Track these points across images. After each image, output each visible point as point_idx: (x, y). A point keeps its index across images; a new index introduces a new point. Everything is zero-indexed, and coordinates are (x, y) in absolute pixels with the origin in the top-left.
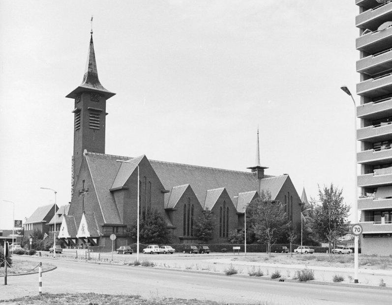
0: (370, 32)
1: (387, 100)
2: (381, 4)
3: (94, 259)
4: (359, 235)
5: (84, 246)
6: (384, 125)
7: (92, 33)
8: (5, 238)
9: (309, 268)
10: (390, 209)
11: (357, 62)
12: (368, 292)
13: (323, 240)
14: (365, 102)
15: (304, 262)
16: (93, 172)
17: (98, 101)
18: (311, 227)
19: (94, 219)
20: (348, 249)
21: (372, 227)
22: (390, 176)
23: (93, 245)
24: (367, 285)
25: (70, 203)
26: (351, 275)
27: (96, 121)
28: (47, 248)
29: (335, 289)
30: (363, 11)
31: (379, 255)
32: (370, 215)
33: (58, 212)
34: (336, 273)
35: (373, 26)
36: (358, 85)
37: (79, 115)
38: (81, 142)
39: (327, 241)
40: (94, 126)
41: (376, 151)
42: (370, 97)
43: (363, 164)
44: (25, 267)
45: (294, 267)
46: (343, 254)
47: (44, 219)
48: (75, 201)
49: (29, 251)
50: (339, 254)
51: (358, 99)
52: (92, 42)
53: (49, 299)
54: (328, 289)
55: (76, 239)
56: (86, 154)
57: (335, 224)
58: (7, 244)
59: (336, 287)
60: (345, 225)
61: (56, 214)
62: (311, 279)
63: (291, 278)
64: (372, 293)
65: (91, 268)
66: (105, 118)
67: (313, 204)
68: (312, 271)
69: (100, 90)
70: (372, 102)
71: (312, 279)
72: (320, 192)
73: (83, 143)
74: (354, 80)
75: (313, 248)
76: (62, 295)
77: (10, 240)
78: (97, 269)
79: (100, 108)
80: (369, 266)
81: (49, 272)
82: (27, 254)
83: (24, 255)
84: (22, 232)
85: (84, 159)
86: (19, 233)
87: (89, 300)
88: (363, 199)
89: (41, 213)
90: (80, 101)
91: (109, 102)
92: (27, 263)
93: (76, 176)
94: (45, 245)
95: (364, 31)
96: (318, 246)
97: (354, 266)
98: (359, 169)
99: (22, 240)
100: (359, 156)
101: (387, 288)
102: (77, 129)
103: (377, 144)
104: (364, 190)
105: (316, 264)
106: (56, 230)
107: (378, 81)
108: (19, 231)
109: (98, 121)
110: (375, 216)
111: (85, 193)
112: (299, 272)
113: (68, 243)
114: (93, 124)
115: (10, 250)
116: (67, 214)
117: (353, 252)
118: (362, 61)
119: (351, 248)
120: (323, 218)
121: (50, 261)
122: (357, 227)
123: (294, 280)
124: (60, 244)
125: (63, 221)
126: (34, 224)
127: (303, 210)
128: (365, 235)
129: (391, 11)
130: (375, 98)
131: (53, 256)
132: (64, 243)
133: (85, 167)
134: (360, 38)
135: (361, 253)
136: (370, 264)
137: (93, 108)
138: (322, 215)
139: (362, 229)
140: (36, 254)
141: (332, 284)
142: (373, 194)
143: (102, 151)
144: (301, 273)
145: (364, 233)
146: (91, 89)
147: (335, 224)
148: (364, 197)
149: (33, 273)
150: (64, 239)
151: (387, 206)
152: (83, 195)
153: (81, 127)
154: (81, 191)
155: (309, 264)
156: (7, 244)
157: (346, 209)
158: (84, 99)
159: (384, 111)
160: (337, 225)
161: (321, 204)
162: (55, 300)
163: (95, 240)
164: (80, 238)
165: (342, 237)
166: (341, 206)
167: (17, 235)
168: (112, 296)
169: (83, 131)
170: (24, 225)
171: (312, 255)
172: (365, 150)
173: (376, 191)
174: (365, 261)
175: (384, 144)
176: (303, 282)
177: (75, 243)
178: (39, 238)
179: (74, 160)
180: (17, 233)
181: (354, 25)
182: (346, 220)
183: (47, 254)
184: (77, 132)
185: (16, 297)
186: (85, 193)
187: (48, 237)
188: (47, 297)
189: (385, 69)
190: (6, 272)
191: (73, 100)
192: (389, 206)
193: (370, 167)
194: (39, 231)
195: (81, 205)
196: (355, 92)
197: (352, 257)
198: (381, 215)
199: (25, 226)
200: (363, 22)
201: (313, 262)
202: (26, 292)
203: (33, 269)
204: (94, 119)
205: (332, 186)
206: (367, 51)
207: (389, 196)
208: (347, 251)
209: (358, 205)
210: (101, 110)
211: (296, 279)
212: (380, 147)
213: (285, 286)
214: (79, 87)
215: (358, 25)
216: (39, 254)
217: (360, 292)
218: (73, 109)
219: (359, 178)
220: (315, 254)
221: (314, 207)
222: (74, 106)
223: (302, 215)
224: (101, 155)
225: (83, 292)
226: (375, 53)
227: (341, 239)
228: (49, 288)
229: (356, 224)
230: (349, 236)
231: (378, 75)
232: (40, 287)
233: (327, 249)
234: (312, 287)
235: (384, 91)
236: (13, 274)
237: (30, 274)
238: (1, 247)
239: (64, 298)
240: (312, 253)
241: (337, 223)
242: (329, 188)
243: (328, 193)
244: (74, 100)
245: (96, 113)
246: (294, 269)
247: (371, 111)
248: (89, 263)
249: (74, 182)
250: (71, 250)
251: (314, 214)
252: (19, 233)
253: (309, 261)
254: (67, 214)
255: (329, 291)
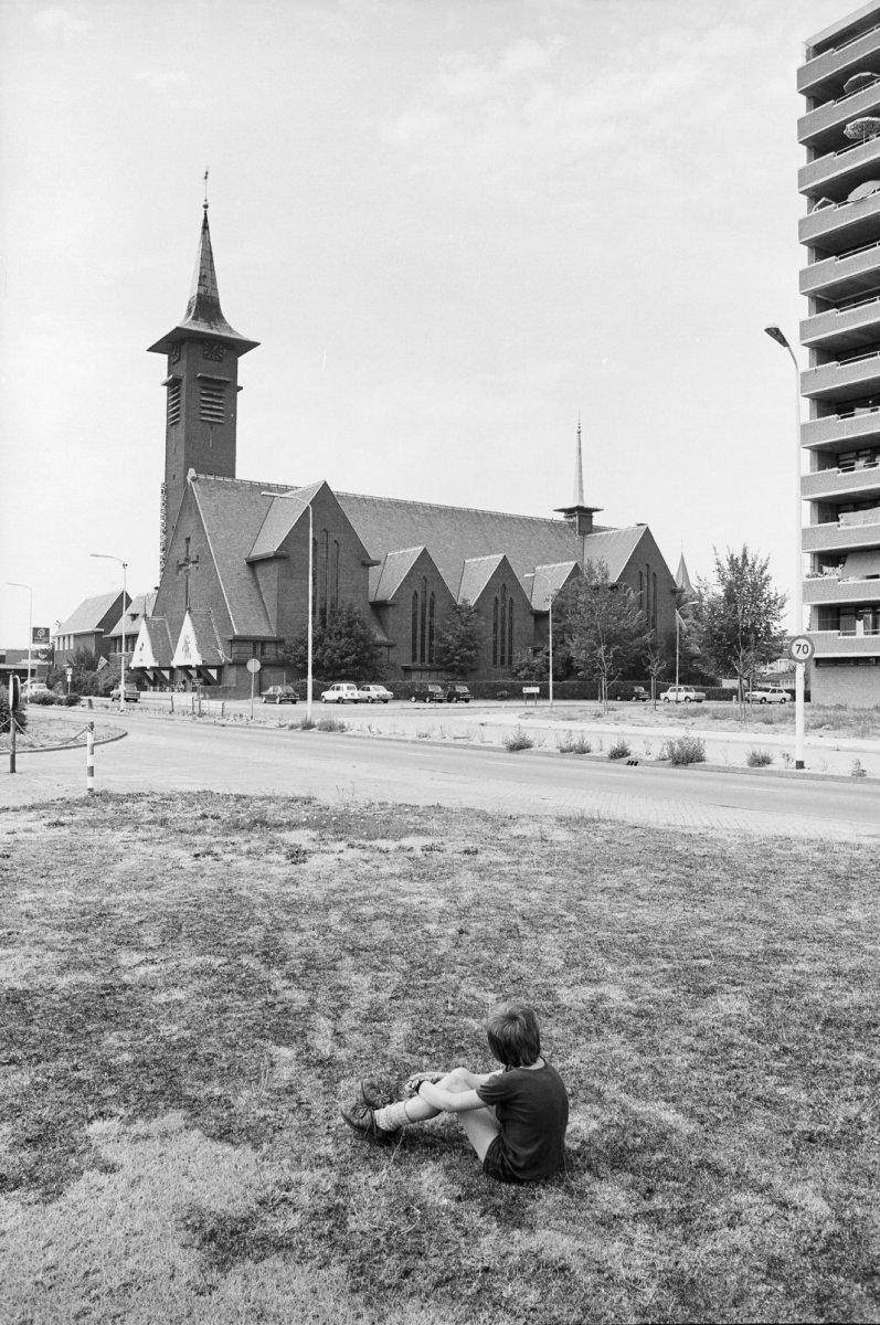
0: (830, 204)
1: (869, 357)
2: (855, 141)
3: (210, 716)
4: (806, 661)
5: (190, 686)
6: (862, 414)
7: (206, 206)
8: (12, 667)
9: (694, 734)
10: (875, 601)
11: (802, 273)
12: (826, 790)
13: (726, 672)
14: (820, 362)
15: (683, 721)
16: (208, 519)
17: (221, 360)
18: (697, 643)
19: (211, 624)
20: (780, 691)
21: (835, 644)
22: (875, 527)
23: (209, 684)
24: (825, 773)
25: (156, 588)
26: (787, 751)
27: (216, 404)
28: (105, 690)
29: (753, 783)
30: (815, 158)
31: (850, 705)
32: (830, 615)
33: (131, 610)
34: (755, 746)
35: (837, 191)
36: (803, 324)
37: (177, 391)
38: (182, 452)
39: (734, 675)
40: (212, 416)
41: (844, 471)
42: (831, 351)
43: (814, 501)
44: (56, 733)
45: (660, 734)
46: (770, 703)
47: (99, 626)
48: (168, 584)
49: (65, 697)
50: (761, 703)
51: (804, 356)
52: (205, 227)
53: (111, 806)
54: (735, 781)
55: (171, 670)
56: (194, 479)
57: (752, 636)
58: (15, 680)
59: (754, 778)
60: (775, 639)
61: (126, 614)
62: (699, 761)
63: (653, 758)
64: (836, 791)
65: (205, 736)
66: (236, 398)
67: (703, 591)
68: (701, 742)
69: (225, 334)
70: (835, 363)
71: (701, 759)
72: (718, 564)
73: (187, 455)
74: (795, 311)
75: (703, 691)
76: (140, 795)
77: (23, 673)
78: (217, 738)
79: (224, 376)
80: (828, 732)
81: (111, 744)
82: (60, 703)
83: (53, 706)
84: (50, 655)
85: (188, 491)
86: (44, 656)
87: (200, 807)
88: (816, 579)
89: (91, 612)
90: (179, 360)
91: (244, 361)
92: (60, 724)
93: (170, 527)
94: (101, 684)
95: (816, 202)
96: (714, 685)
97: (794, 731)
98: (807, 512)
99: (49, 671)
100: (805, 483)
101: (869, 781)
102: (173, 423)
103: (847, 456)
104: (817, 560)
105: (710, 727)
106: (127, 650)
107: (849, 315)
108: (44, 652)
109: (219, 404)
110: (842, 619)
111: (191, 566)
112: (671, 744)
113: (152, 678)
114: (208, 412)
115: (23, 695)
116: (150, 614)
117: (794, 699)
118: (812, 269)
119: (787, 691)
120: (725, 622)
121: (112, 720)
122: (802, 642)
123: (661, 763)
124: (134, 681)
125: (142, 629)
126: (77, 636)
127: (679, 604)
128: (819, 661)
129: (879, 158)
130: (842, 352)
131: (118, 708)
132: (143, 679)
133: (190, 508)
134: (807, 219)
135: (809, 701)
136: (831, 727)
137: (208, 376)
138: (724, 616)
139: (813, 648)
140: (82, 703)
141: (744, 772)
142: (838, 570)
143: (230, 471)
144: (677, 746)
145: (816, 655)
146: (203, 333)
147: (752, 636)
148: (817, 576)
149: (74, 747)
150: (144, 669)
151: (870, 595)
152: (186, 571)
153: (183, 419)
154: (181, 562)
155: (694, 727)
156: (15, 681)
157: (776, 603)
158: (188, 355)
159: (862, 383)
160: (757, 639)
161: (720, 591)
162: (123, 807)
163: (214, 673)
164: (180, 667)
165: (768, 666)
166: (765, 596)
167: (38, 662)
168: (251, 798)
169: (187, 426)
170: (54, 637)
171: (700, 705)
172: (820, 469)
173: (844, 563)
174: (820, 719)
175: (862, 456)
176: (680, 766)
177: (168, 678)
178: (88, 668)
179: (166, 491)
180: (37, 657)
181: (795, 189)
182: (777, 627)
183: (106, 703)
184: (173, 430)
185: (37, 801)
186: (191, 566)
187: (107, 664)
188: (106, 801)
189: (865, 287)
190: (14, 743)
191: (165, 357)
192: (873, 595)
193: (830, 509)
194: (87, 653)
195: (182, 593)
196: (798, 339)
197: (791, 710)
198: (856, 616)
199: (56, 640)
200: (815, 183)
201: (702, 721)
202: (58, 788)
203: (75, 738)
204: (211, 400)
205: (745, 550)
206: (825, 247)
207: (874, 574)
208: (779, 696)
209: (804, 594)
210: (227, 379)
211: (664, 759)
212: (853, 464)
213: (641, 776)
214: (177, 328)
215: (803, 189)
216: (87, 703)
217: (809, 788)
218: (165, 377)
219: (805, 532)
220: (706, 704)
221: (705, 599)
222: (166, 371)
223: (678, 616)
224: (226, 480)
225: (186, 788)
226: (842, 253)
227: (765, 670)
228: (110, 781)
229: (799, 637)
230: (783, 664)
231: (849, 300)
232: (89, 779)
233: (734, 692)
234: (701, 778)
235: (863, 337)
236: (29, 749)
237: (67, 748)
238: (3, 687)
239: (145, 804)
240: (699, 701)
241: (756, 634)
242: (738, 554)
243: (737, 566)
244: (166, 356)
245: (216, 387)
246: (659, 737)
247: (833, 383)
248: (199, 723)
249: (166, 541)
250: (159, 694)
251: (705, 613)
252: (44, 656)
253: (694, 720)
254: (150, 614)
255: (739, 787)
